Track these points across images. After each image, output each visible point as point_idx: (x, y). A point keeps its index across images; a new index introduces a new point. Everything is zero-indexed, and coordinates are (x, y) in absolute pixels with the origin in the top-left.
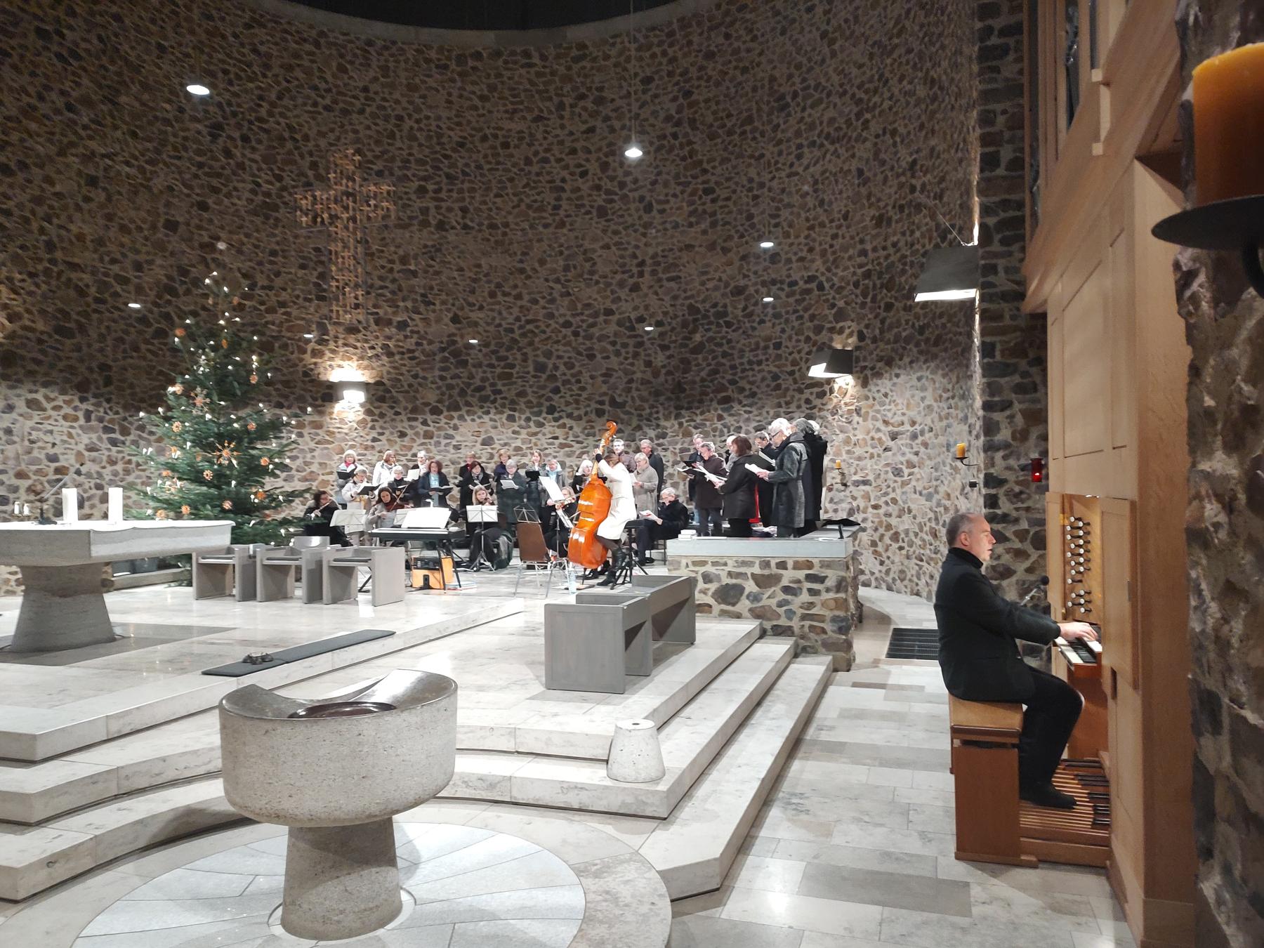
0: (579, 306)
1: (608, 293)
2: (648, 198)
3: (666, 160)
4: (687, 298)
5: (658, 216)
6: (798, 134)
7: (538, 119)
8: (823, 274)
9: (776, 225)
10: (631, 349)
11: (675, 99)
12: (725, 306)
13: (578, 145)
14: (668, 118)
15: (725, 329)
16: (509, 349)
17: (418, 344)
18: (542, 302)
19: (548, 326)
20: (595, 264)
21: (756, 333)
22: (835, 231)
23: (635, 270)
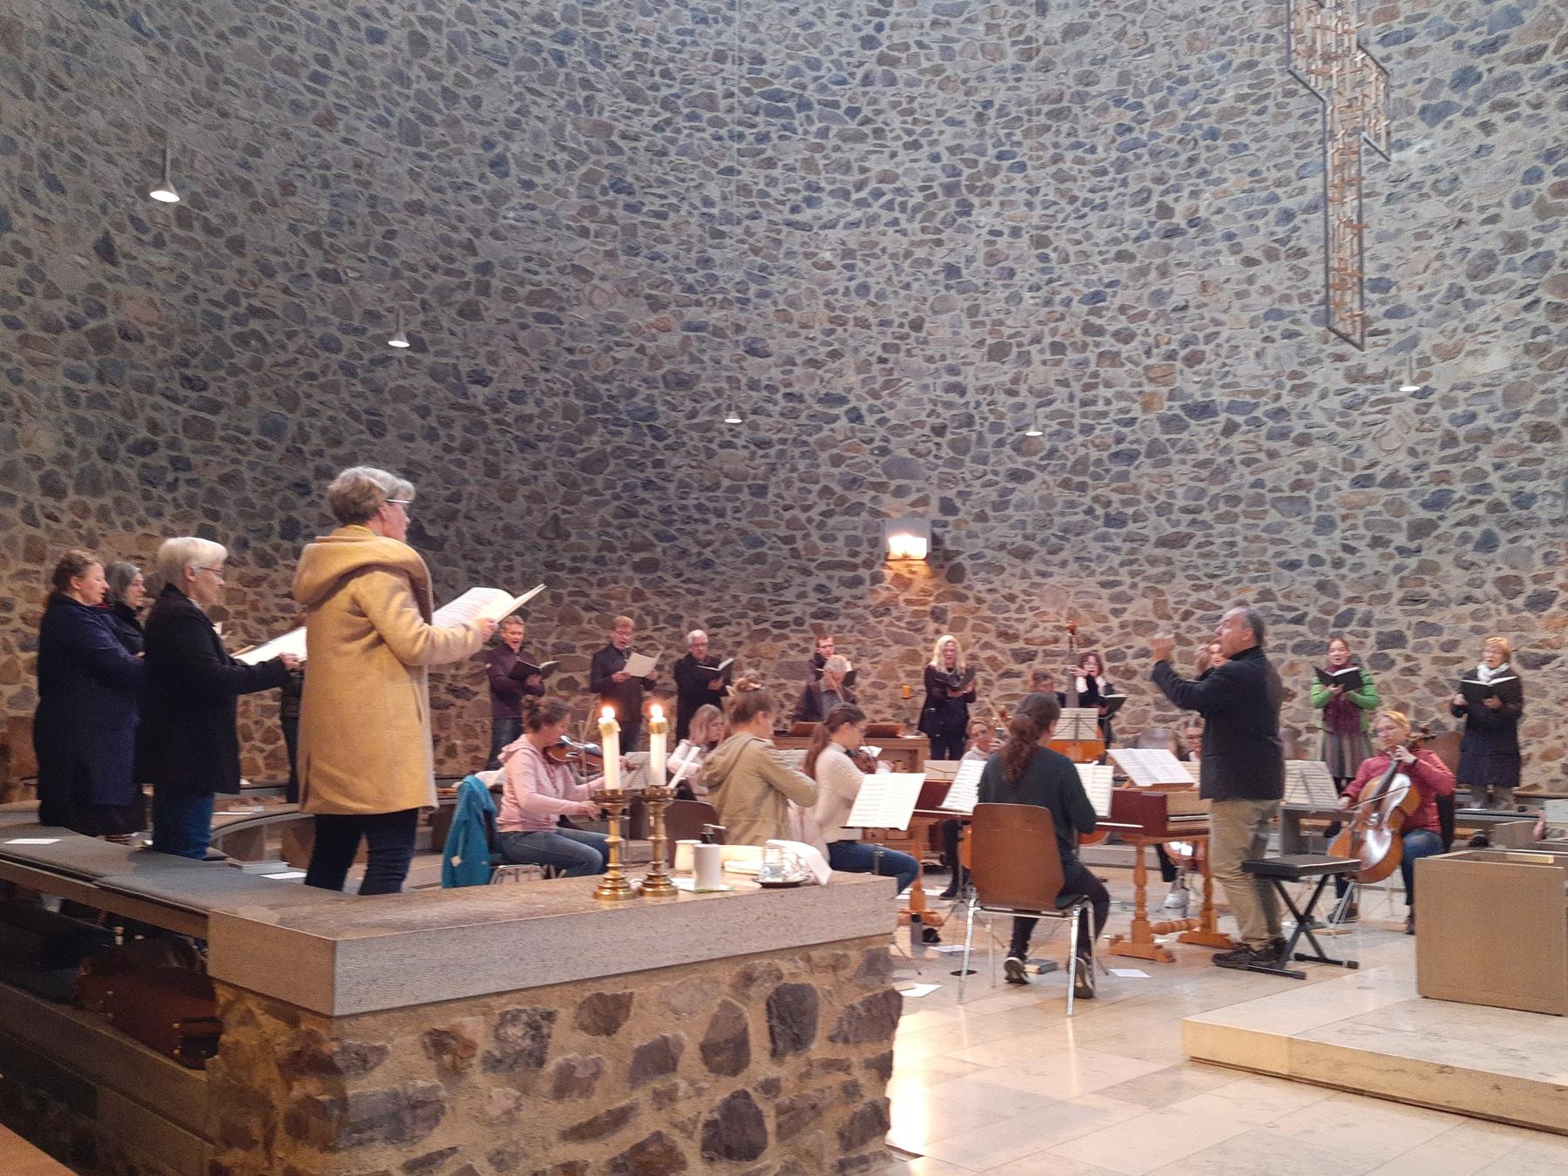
0: (357, 312)
1: (417, 304)
2: (499, 149)
3: (540, 94)
4: (572, 365)
5: (518, 190)
6: (809, 165)
8: (860, 398)
9: (764, 295)
10: (457, 432)
12: (650, 399)
14: (544, 19)
15: (649, 440)
16: (211, 364)
17: (24, 286)
18: (282, 278)
19: (291, 335)
20: (391, 234)
21: (715, 462)
22: (889, 340)
23: (471, 276)
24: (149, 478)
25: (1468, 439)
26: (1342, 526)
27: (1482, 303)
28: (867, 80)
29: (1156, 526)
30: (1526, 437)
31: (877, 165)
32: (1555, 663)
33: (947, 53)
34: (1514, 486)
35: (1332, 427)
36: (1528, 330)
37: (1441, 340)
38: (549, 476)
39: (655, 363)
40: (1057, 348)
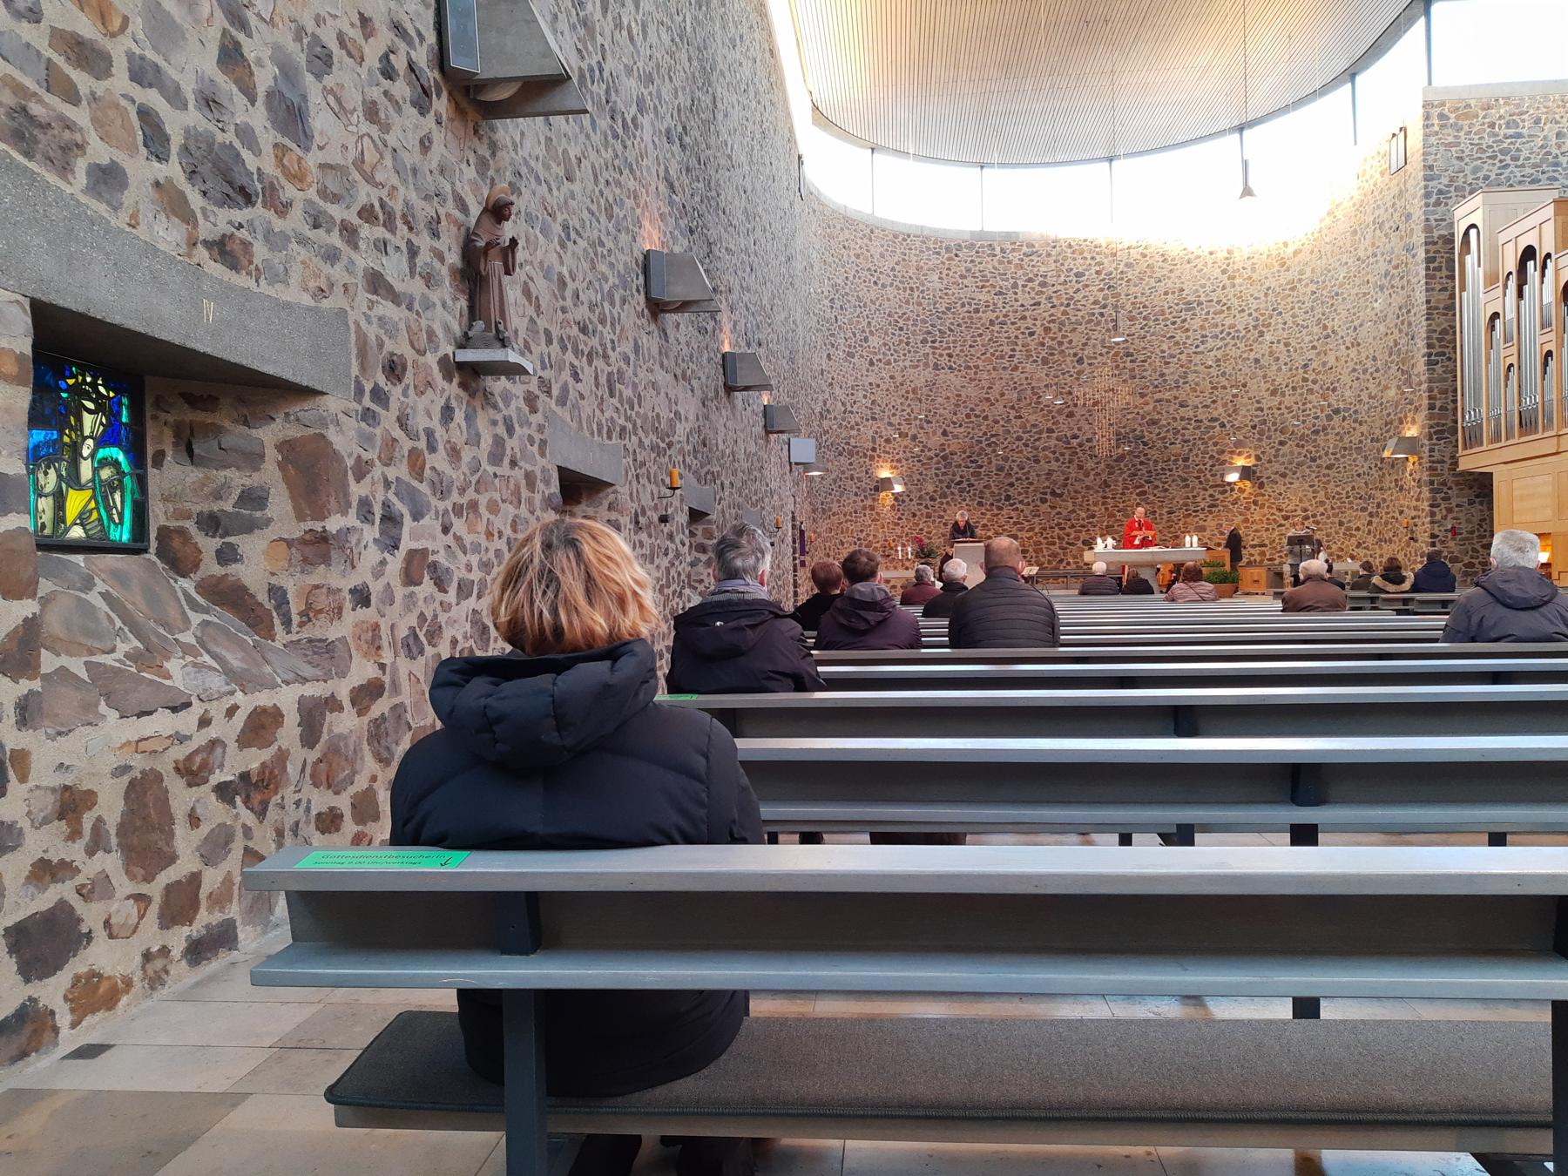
6: (1202, 327)
7: (1001, 293)
11: (1101, 290)
13: (1027, 314)
14: (1095, 303)
24: (962, 490)
28: (1224, 288)
29: (1324, 462)
31: (1228, 322)
33: (1254, 270)
38: (1102, 466)
39: (1143, 417)
40: (1294, 388)
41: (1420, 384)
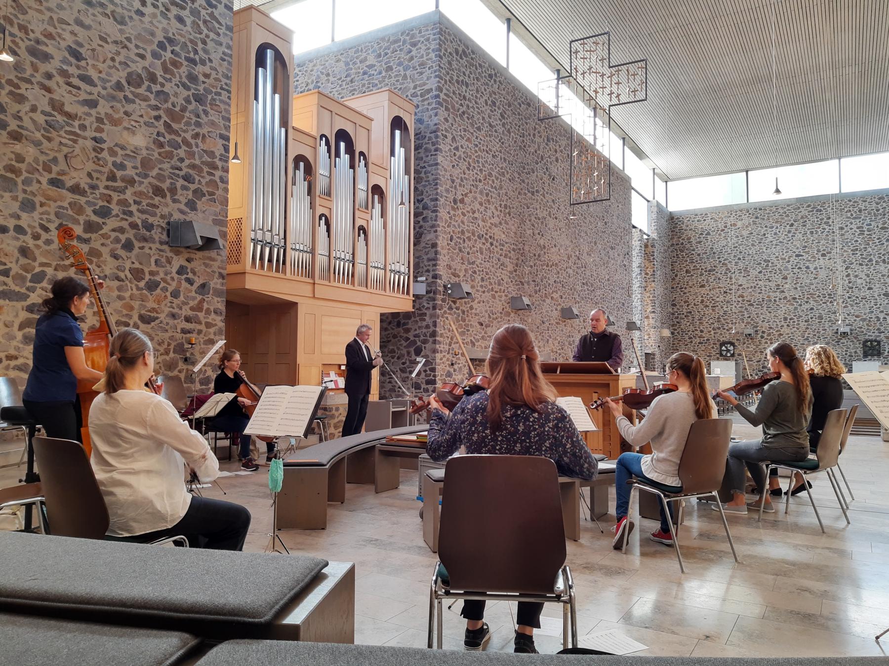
25: (123, 180)
26: (39, 209)
27: (133, 102)
30: (151, 191)
32: (157, 321)
34: (144, 216)
35: (38, 135)
36: (156, 130)
37: (110, 111)
41: (216, 168)
